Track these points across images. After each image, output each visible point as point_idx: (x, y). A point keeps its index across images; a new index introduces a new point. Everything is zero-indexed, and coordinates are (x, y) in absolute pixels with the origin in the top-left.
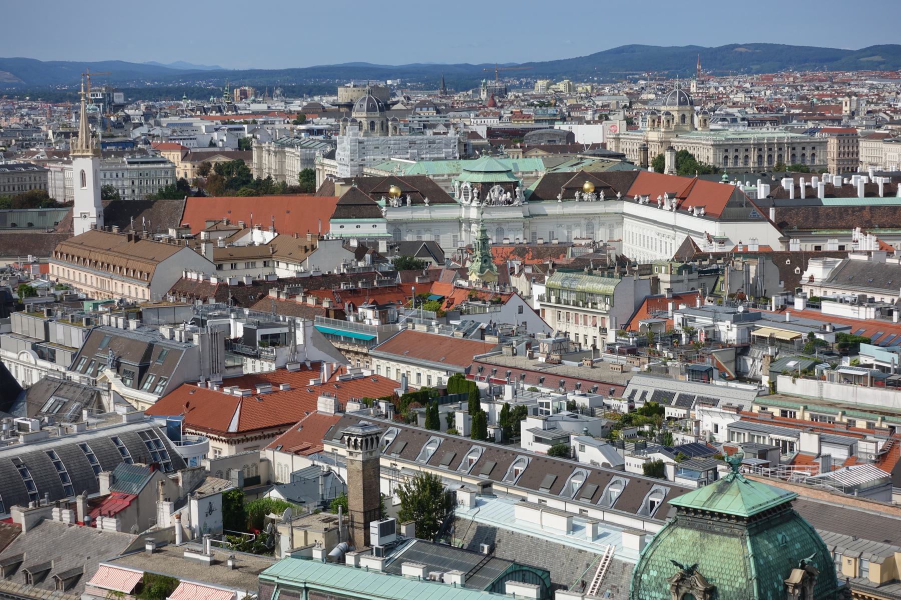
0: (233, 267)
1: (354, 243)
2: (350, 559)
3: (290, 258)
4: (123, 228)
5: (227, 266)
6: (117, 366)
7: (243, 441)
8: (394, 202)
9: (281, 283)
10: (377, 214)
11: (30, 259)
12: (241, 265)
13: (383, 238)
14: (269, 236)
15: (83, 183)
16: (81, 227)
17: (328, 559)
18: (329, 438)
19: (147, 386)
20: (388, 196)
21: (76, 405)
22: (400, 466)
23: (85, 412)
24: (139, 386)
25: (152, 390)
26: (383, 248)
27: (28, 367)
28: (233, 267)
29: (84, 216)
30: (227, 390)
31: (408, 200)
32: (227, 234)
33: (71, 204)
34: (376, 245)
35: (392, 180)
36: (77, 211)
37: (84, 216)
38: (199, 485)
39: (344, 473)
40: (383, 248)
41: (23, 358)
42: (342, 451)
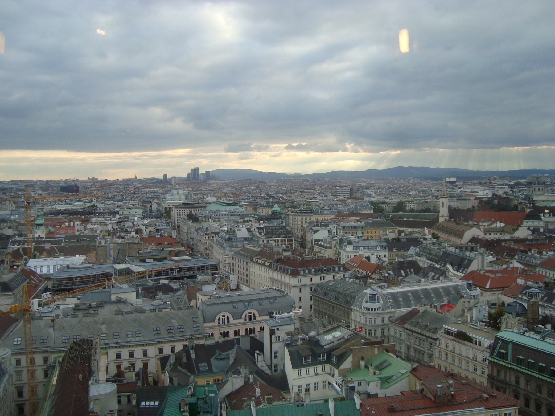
0: (490, 234)
1: (532, 228)
2: (527, 334)
3: (509, 233)
4: (455, 220)
5: (488, 234)
6: (452, 264)
7: (491, 291)
8: (547, 215)
9: (506, 240)
10: (540, 219)
11: (426, 228)
12: (492, 234)
13: (542, 227)
14: (502, 225)
15: (443, 206)
16: (441, 220)
17: (519, 333)
18: (521, 293)
19: (460, 271)
20: (544, 213)
21: (438, 275)
22: (546, 305)
23: (441, 278)
24: (458, 271)
25: (462, 272)
26: (542, 230)
27: (423, 262)
28: (490, 234)
29: (443, 216)
30: (487, 274)
31: (551, 214)
32: (489, 223)
33: (439, 212)
34: (539, 229)
35: (546, 208)
36: (440, 214)
37: (443, 216)
38: (477, 303)
39: (526, 305)
40: (542, 230)
41: (422, 259)
42: (525, 298)
